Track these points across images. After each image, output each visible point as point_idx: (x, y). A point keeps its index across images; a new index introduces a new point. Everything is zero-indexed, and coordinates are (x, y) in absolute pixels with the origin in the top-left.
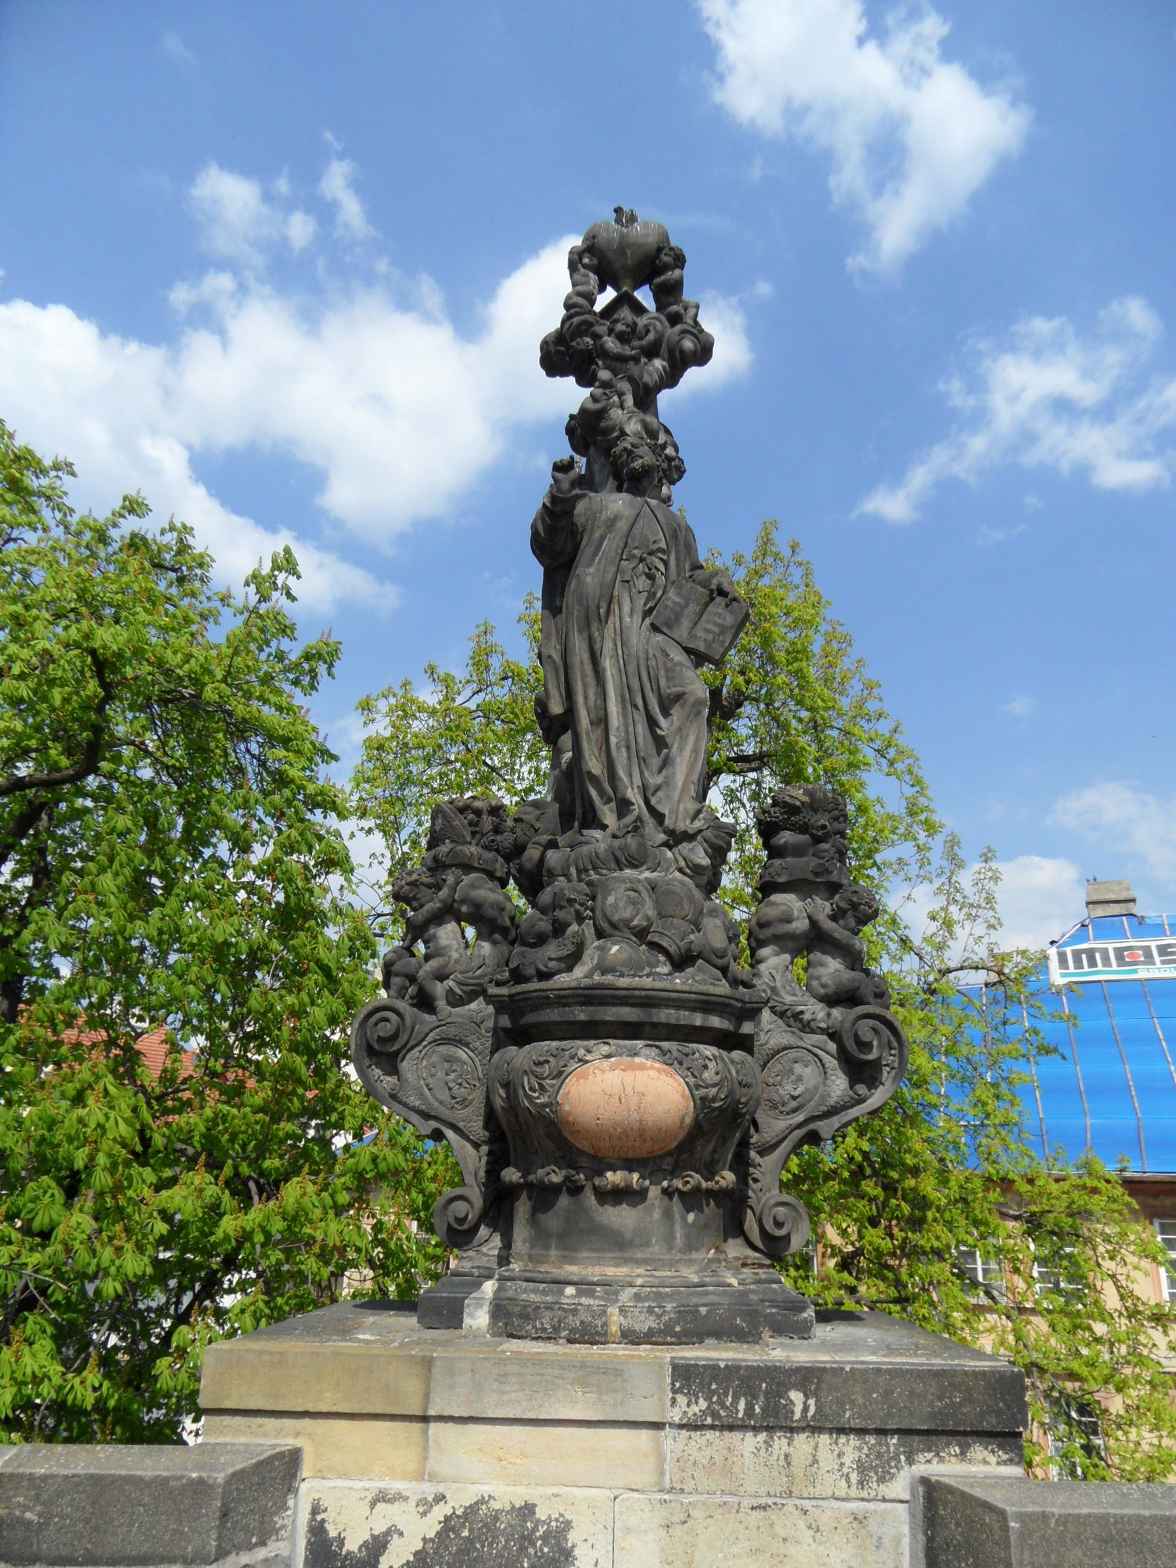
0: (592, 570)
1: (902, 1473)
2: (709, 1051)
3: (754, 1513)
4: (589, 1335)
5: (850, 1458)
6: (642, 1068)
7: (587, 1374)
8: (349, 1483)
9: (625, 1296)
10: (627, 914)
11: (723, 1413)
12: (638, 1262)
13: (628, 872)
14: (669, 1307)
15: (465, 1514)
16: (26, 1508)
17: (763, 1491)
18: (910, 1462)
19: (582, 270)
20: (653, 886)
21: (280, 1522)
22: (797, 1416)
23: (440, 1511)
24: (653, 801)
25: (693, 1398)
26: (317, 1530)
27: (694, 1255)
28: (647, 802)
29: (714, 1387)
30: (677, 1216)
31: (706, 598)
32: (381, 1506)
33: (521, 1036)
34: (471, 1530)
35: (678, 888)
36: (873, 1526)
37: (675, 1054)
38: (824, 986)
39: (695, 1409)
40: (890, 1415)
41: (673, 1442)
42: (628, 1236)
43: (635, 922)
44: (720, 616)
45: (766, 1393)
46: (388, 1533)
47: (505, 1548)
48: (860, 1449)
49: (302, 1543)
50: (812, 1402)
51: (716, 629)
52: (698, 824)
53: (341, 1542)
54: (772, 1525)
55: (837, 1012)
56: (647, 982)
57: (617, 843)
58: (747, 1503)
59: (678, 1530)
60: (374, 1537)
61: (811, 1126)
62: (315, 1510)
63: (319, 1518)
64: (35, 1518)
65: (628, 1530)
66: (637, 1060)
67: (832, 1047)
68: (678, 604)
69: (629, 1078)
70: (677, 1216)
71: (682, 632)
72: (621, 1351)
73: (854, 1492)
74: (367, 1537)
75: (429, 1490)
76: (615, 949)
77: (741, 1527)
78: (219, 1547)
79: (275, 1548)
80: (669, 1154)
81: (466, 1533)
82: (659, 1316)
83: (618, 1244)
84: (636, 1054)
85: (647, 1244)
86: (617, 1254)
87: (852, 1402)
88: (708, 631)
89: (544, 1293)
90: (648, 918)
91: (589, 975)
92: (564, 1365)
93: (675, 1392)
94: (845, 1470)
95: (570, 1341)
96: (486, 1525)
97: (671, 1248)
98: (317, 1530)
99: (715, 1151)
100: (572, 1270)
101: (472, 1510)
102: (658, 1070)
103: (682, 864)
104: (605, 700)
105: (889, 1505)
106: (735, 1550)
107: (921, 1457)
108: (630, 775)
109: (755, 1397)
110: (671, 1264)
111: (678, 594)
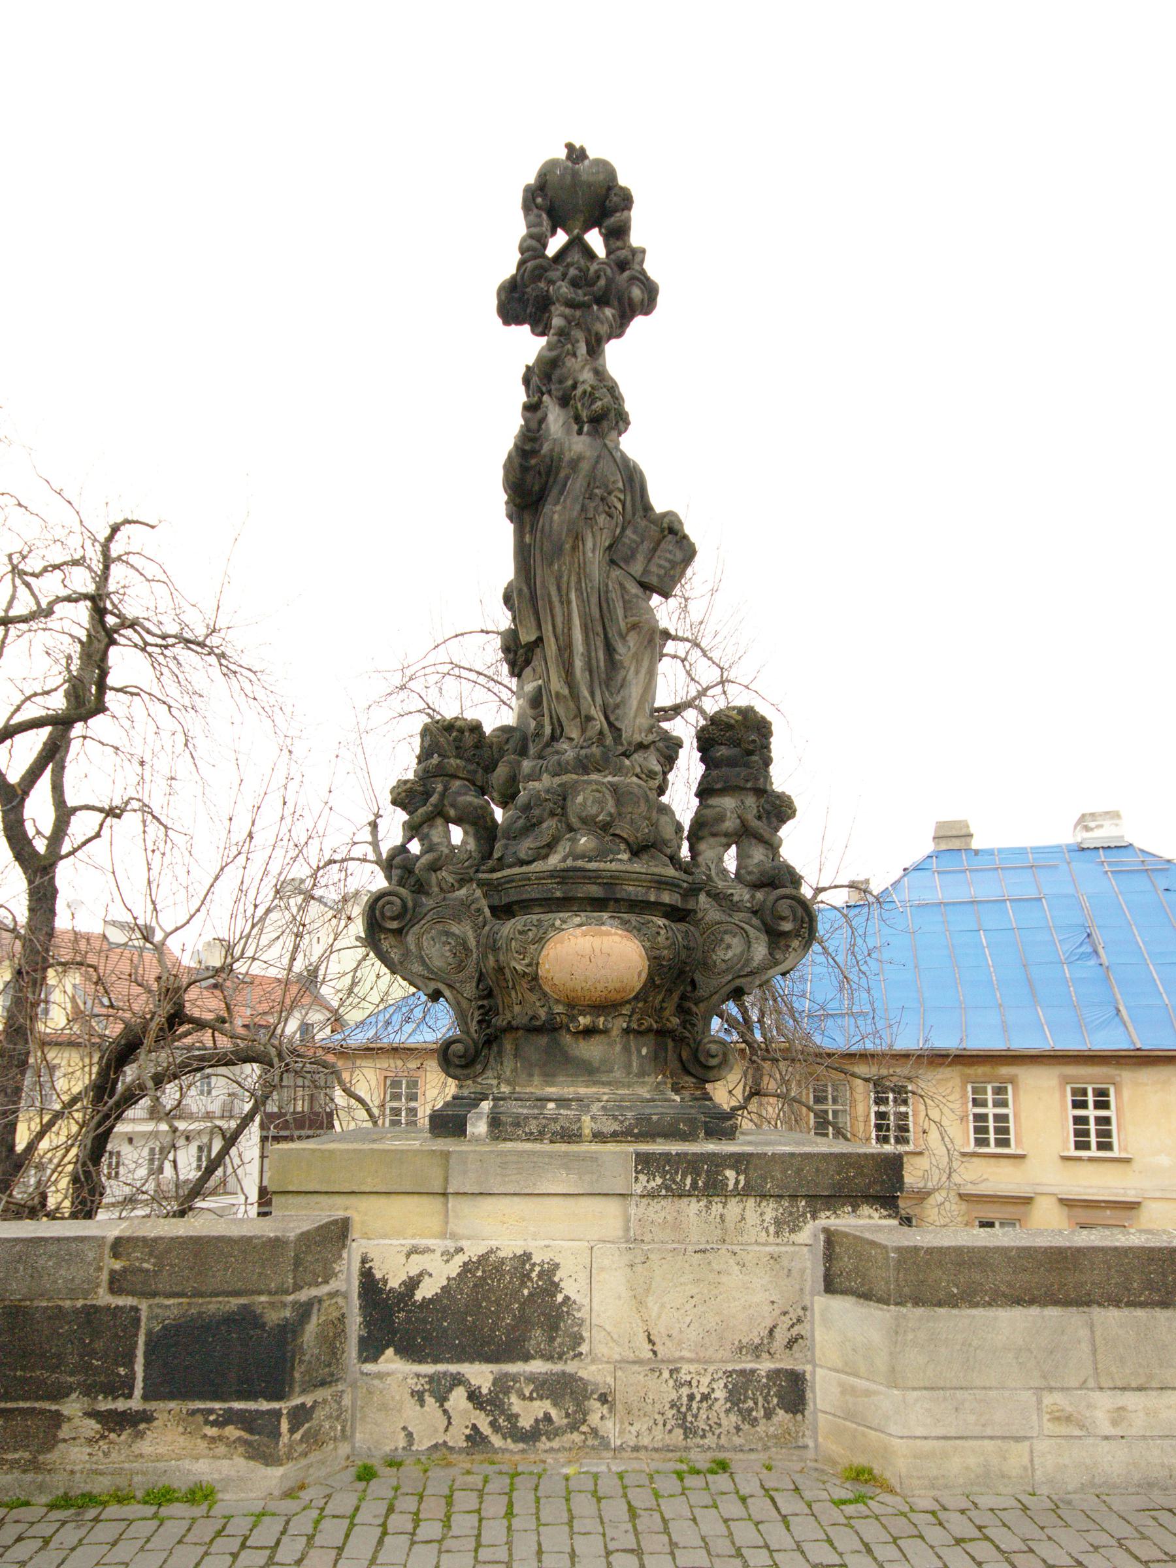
0: (558, 508)
1: (808, 1226)
2: (661, 922)
3: (698, 1255)
4: (569, 1136)
5: (770, 1215)
6: (608, 934)
7: (568, 1162)
8: (390, 1242)
9: (595, 1108)
10: (593, 810)
11: (674, 1187)
12: (604, 1084)
13: (594, 777)
14: (629, 1115)
15: (479, 1261)
16: (144, 1261)
17: (703, 1240)
18: (814, 1218)
19: (535, 211)
20: (615, 789)
21: (337, 1269)
22: (731, 1187)
23: (460, 1259)
24: (612, 718)
25: (651, 1176)
26: (367, 1276)
27: (647, 1079)
28: (607, 718)
29: (667, 1168)
30: (633, 1049)
31: (657, 535)
32: (414, 1257)
33: (503, 911)
34: (483, 1271)
35: (636, 790)
36: (785, 1262)
37: (634, 923)
38: (750, 873)
39: (653, 1184)
40: (800, 1185)
41: (636, 1210)
42: (596, 1065)
43: (600, 818)
44: (670, 552)
45: (707, 1171)
46: (421, 1274)
47: (509, 1282)
48: (777, 1210)
49: (356, 1283)
50: (742, 1178)
51: (667, 565)
52: (651, 738)
53: (385, 1282)
54: (709, 1263)
55: (759, 895)
56: (613, 866)
57: (583, 752)
58: (690, 1248)
59: (639, 1268)
60: (410, 1278)
61: (738, 982)
62: (364, 1261)
63: (367, 1266)
64: (150, 1267)
65: (602, 1269)
66: (604, 928)
67: (755, 921)
68: (635, 541)
69: (597, 942)
70: (633, 1049)
71: (637, 568)
72: (595, 1147)
73: (771, 1239)
74: (404, 1277)
75: (451, 1245)
76: (583, 840)
77: (687, 1266)
78: (295, 1284)
79: (333, 1285)
80: (628, 1002)
81: (479, 1274)
82: (622, 1122)
83: (588, 1071)
84: (603, 924)
85: (611, 1071)
87: (772, 1177)
88: (660, 566)
89: (530, 1107)
90: (611, 815)
91: (564, 860)
92: (551, 1155)
93: (637, 1172)
94: (765, 1225)
95: (552, 1142)
96: (495, 1268)
97: (629, 1074)
98: (367, 1276)
99: (663, 1001)
100: (551, 1090)
101: (483, 1258)
103: (638, 770)
104: (570, 629)
105: (797, 1248)
106: (682, 1280)
107: (822, 1215)
108: (592, 694)
109: (698, 1175)
110: (629, 1085)
111: (635, 532)
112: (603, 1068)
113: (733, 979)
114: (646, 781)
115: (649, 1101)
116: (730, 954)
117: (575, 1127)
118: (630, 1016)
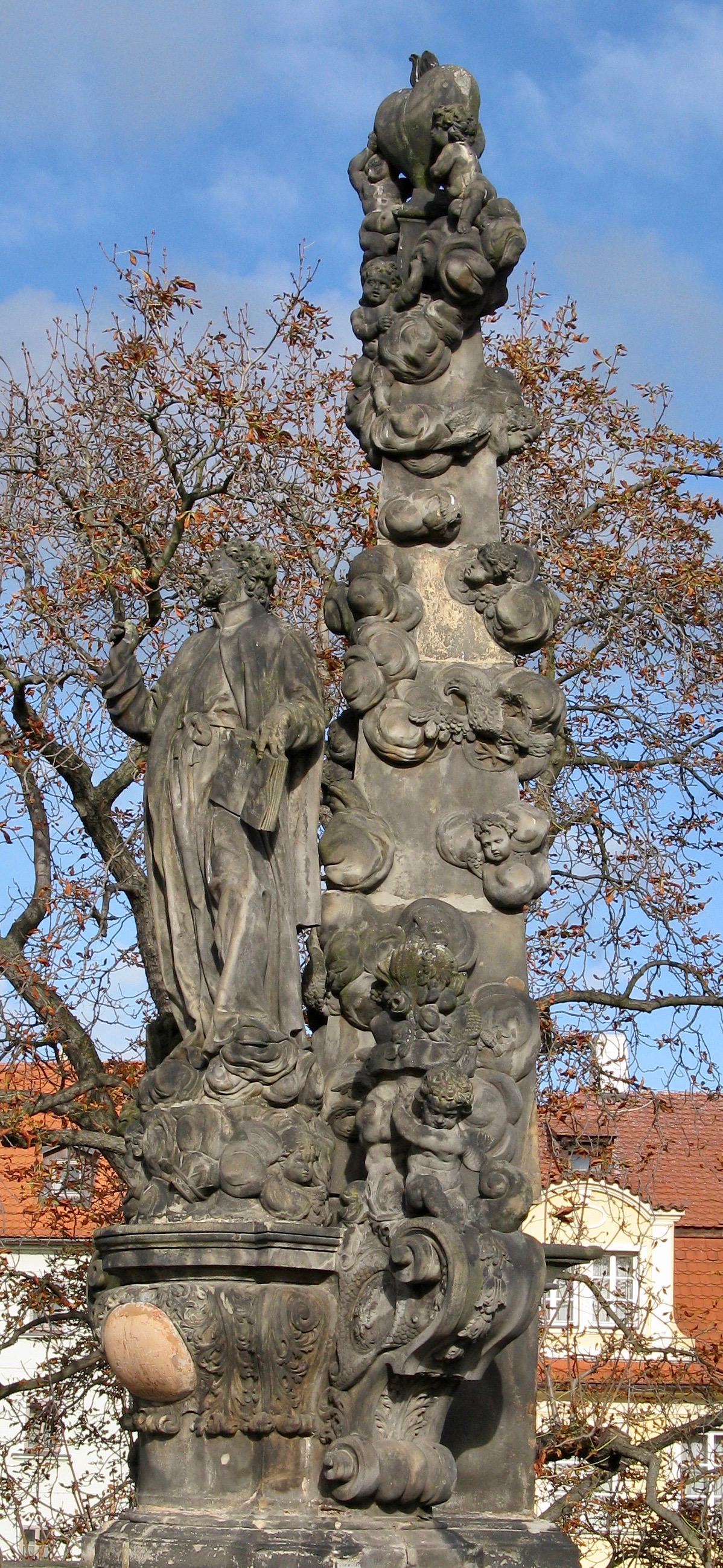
27: (229, 1496)
30: (208, 1457)
66: (139, 1304)
82: (155, 1550)
86: (161, 1494)
97: (202, 1489)
102: (149, 1315)
112: (174, 1482)
113: (379, 1354)
114: (218, 1100)
115: (221, 1524)
116: (374, 1316)
117: (118, 1555)
118: (200, 1413)
